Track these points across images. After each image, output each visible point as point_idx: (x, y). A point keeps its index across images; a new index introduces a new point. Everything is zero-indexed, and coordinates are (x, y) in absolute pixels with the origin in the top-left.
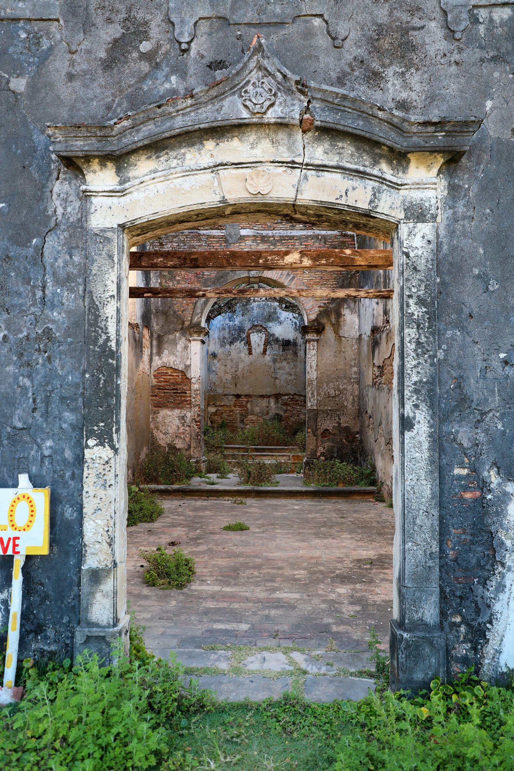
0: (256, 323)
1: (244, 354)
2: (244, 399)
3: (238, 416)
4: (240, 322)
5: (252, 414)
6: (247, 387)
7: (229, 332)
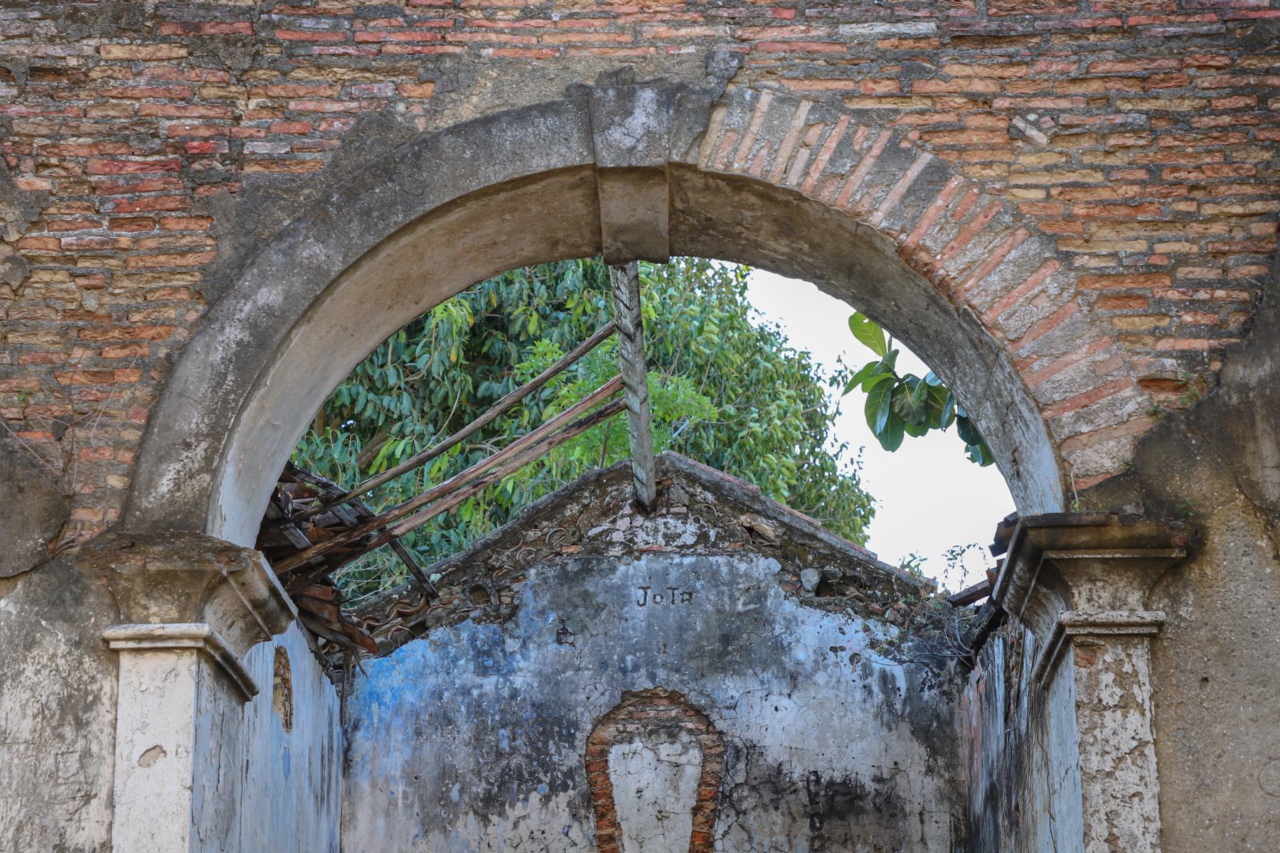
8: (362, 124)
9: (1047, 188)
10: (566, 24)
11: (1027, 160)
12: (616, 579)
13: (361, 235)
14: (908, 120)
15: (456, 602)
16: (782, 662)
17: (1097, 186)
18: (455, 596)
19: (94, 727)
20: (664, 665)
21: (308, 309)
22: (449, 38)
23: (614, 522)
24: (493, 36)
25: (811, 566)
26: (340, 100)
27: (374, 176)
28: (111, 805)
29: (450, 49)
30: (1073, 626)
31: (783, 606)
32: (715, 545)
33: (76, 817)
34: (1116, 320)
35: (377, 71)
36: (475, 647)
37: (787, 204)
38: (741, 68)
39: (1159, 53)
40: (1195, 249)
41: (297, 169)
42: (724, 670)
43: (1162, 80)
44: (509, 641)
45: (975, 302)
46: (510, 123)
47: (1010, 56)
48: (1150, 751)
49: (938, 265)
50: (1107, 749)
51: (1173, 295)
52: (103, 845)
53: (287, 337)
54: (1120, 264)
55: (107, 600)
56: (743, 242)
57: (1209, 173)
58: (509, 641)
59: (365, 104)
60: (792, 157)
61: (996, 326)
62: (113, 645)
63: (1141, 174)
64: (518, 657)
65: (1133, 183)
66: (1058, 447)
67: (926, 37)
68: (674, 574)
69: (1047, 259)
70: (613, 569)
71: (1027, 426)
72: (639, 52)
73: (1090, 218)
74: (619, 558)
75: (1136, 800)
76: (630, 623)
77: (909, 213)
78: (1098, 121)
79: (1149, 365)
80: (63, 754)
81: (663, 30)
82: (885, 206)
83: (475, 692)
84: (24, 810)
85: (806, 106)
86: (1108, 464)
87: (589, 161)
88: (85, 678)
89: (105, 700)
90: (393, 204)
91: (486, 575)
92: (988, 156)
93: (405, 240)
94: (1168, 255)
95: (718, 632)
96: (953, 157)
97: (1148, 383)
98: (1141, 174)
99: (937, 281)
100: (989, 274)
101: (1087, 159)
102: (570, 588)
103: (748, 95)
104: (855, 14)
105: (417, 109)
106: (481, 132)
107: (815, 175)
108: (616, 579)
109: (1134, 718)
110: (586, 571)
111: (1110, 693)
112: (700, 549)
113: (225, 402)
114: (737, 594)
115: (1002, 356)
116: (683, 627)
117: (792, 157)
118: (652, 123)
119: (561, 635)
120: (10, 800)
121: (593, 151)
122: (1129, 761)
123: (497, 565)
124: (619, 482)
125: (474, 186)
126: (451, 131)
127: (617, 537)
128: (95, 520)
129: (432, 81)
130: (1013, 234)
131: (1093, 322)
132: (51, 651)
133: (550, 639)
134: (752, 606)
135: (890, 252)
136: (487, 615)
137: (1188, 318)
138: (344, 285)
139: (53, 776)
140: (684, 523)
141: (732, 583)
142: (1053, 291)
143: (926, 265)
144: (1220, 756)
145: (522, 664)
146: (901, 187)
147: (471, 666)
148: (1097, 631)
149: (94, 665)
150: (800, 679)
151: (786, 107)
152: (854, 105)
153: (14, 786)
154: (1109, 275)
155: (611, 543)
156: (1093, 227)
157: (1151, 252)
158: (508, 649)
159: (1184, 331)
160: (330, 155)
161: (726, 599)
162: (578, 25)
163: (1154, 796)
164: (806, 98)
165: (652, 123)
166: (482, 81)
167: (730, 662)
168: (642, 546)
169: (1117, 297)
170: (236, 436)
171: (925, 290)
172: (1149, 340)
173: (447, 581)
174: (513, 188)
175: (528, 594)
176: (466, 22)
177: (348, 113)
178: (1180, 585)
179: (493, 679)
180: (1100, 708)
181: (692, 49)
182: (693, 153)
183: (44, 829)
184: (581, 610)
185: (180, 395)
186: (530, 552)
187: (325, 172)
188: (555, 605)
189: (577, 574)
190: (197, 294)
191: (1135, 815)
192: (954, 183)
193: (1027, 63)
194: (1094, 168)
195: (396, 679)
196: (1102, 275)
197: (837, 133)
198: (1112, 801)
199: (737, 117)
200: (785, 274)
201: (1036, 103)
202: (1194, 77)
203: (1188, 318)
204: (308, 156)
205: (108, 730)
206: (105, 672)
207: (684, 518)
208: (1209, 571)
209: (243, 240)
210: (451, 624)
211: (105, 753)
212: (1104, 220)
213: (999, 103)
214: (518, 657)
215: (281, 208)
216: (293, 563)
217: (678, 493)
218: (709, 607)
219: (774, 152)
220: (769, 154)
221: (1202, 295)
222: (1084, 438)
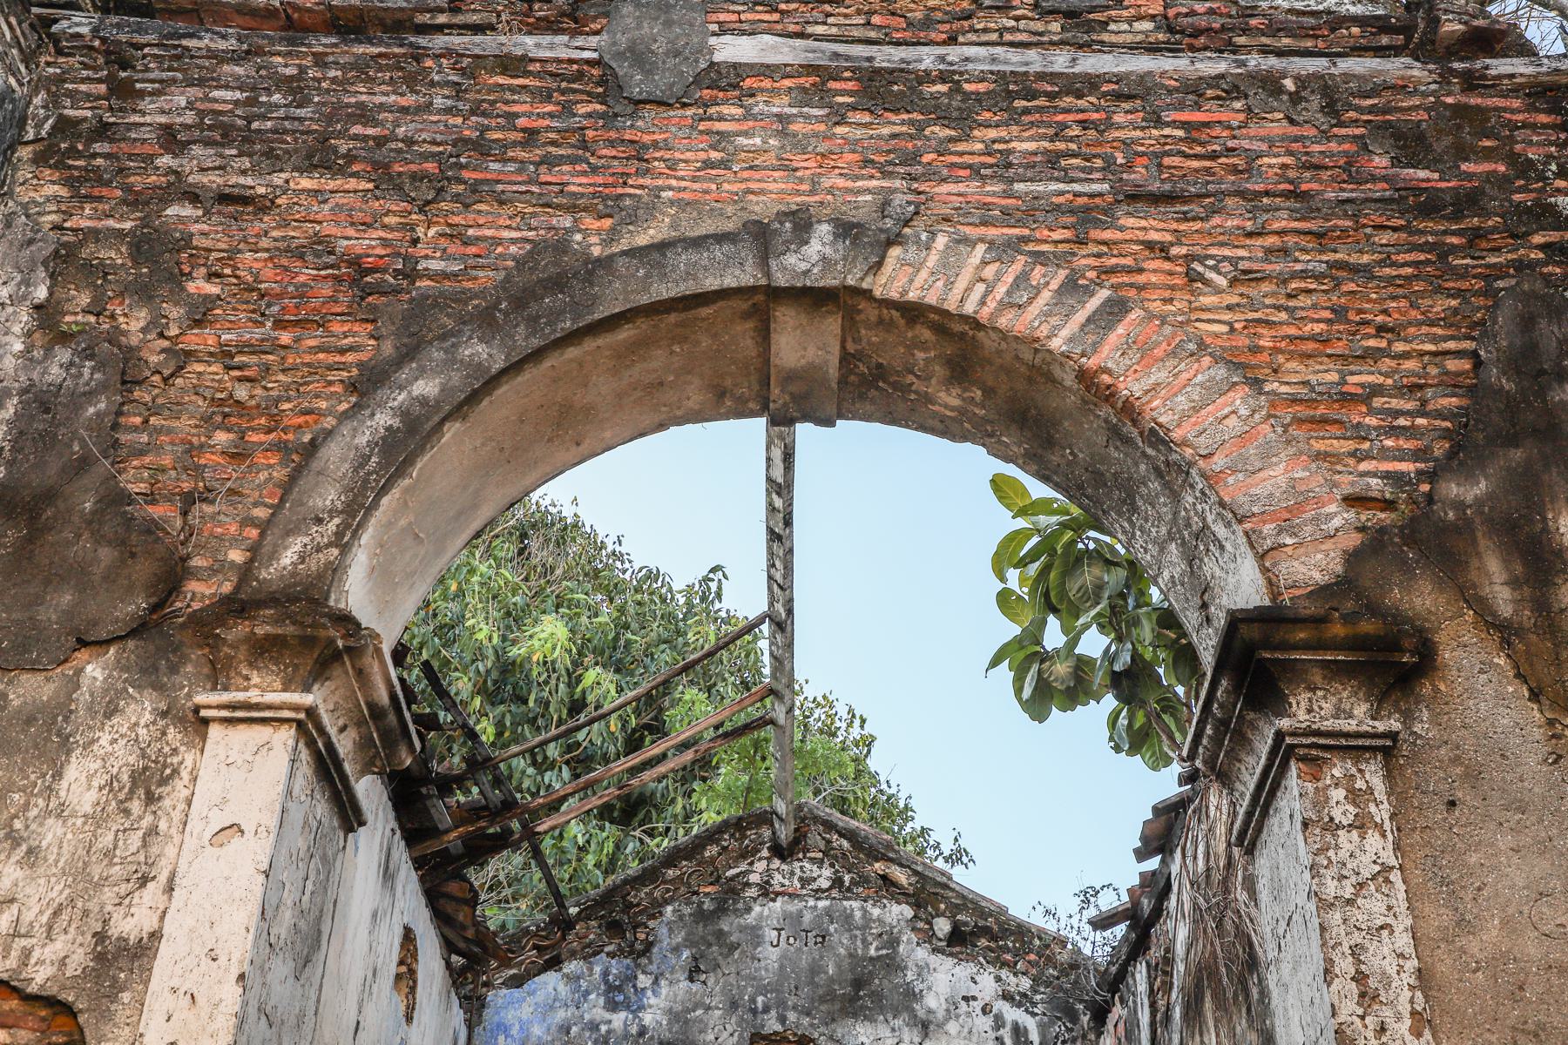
8: (537, 247)
9: (1230, 324)
10: (746, 174)
11: (1206, 300)
12: (750, 919)
13: (527, 338)
14: (1084, 262)
15: (592, 936)
16: (913, 1010)
17: (1281, 323)
18: (592, 931)
19: (167, 803)
20: (794, 1008)
21: (465, 405)
22: (630, 182)
23: (751, 864)
24: (674, 183)
25: (943, 915)
26: (518, 229)
27: (545, 288)
28: (170, 889)
29: (632, 191)
30: (1293, 734)
31: (915, 953)
32: (849, 890)
33: (127, 901)
34: (1312, 442)
35: (558, 207)
36: (607, 982)
37: (963, 335)
38: (917, 213)
39: (1333, 214)
40: (1390, 381)
41: (470, 285)
42: (855, 1015)
43: (1339, 237)
44: (641, 977)
45: (1162, 420)
46: (686, 249)
47: (1184, 213)
48: (1395, 876)
49: (1122, 386)
50: (1345, 872)
51: (1371, 421)
52: (152, 935)
53: (438, 428)
54: (1312, 390)
55: (206, 670)
56: (913, 397)
57: (1396, 316)
58: (641, 977)
59: (542, 232)
60: (968, 290)
61: (1185, 443)
62: (203, 713)
63: (1327, 314)
64: (649, 993)
65: (1318, 321)
66: (1261, 557)
67: (1101, 195)
68: (808, 917)
69: (1235, 384)
70: (749, 910)
71: (1222, 548)
72: (817, 198)
73: (1276, 350)
74: (755, 900)
75: (1385, 933)
76: (763, 964)
77: (1091, 339)
78: (1277, 267)
79: (1352, 484)
80: (125, 830)
81: (841, 182)
82: (1065, 333)
83: (604, 1028)
84: (67, 891)
85: (981, 248)
86: (1317, 576)
87: (763, 282)
88: (167, 749)
89: (185, 774)
90: (563, 312)
91: (623, 911)
92: (1167, 294)
93: (572, 352)
94: (1362, 385)
95: (850, 976)
96: (1132, 293)
97: (1352, 501)
98: (1327, 314)
99: (1120, 404)
100: (1175, 395)
101: (1268, 301)
102: (705, 926)
103: (924, 236)
104: (1029, 174)
105: (594, 240)
106: (656, 256)
107: (992, 305)
108: (750, 919)
109: (1373, 841)
110: (721, 910)
111: (1342, 812)
112: (835, 893)
113: (366, 481)
114: (870, 939)
115: (1193, 472)
116: (815, 969)
117: (968, 290)
118: (828, 251)
119: (693, 973)
120: (53, 880)
121: (768, 274)
122: (1372, 887)
123: (635, 901)
124: (758, 826)
125: (645, 300)
126: (624, 253)
127: (754, 878)
128: (208, 592)
129: (611, 216)
130: (1198, 361)
131: (1288, 442)
132: (133, 720)
133: (682, 976)
134: (884, 952)
135: (1069, 380)
136: (621, 950)
137: (1389, 443)
138: (504, 388)
139: (109, 854)
140: (820, 868)
141: (865, 927)
142: (1244, 412)
143: (1109, 387)
144: (1479, 889)
145: (653, 1001)
146: (1081, 316)
147: (602, 1001)
148: (1322, 741)
149: (179, 736)
150: (932, 1027)
151: (961, 247)
152: (1031, 247)
153: (61, 864)
154: (1301, 400)
155: (748, 884)
156: (1281, 359)
157: (1343, 382)
158: (640, 985)
159: (1384, 455)
160: (503, 273)
161: (859, 943)
162: (757, 175)
163: (1406, 930)
164: (982, 240)
165: (828, 251)
166: (660, 218)
167: (861, 1007)
168: (778, 888)
169: (1312, 420)
170: (373, 520)
171: (1106, 421)
172: (1351, 461)
173: (585, 915)
174: (686, 309)
175: (664, 930)
176: (648, 170)
177: (526, 240)
178: (1412, 699)
179: (623, 1015)
180: (1332, 826)
181: (869, 198)
182: (869, 279)
183: (86, 913)
184: (715, 948)
185: (319, 473)
186: (668, 890)
187: (495, 287)
188: (689, 942)
189: (713, 912)
190: (352, 387)
191: (1386, 951)
192: (1133, 315)
193: (1202, 219)
194: (1278, 308)
195: (526, 1011)
196: (1295, 400)
197: (1017, 267)
198: (1356, 933)
199: (912, 253)
200: (953, 438)
201: (1213, 251)
202: (1371, 236)
203: (1389, 443)
204: (481, 274)
205: (182, 806)
206: (190, 745)
207: (820, 863)
208: (1442, 687)
209: (405, 340)
210: (585, 958)
211: (173, 831)
212: (1290, 352)
213: (1174, 251)
214: (649, 993)
215: (448, 315)
216: (431, 847)
217: (815, 838)
218: (842, 951)
219: (949, 285)
220: (945, 285)
221: (1402, 422)
222: (1289, 550)
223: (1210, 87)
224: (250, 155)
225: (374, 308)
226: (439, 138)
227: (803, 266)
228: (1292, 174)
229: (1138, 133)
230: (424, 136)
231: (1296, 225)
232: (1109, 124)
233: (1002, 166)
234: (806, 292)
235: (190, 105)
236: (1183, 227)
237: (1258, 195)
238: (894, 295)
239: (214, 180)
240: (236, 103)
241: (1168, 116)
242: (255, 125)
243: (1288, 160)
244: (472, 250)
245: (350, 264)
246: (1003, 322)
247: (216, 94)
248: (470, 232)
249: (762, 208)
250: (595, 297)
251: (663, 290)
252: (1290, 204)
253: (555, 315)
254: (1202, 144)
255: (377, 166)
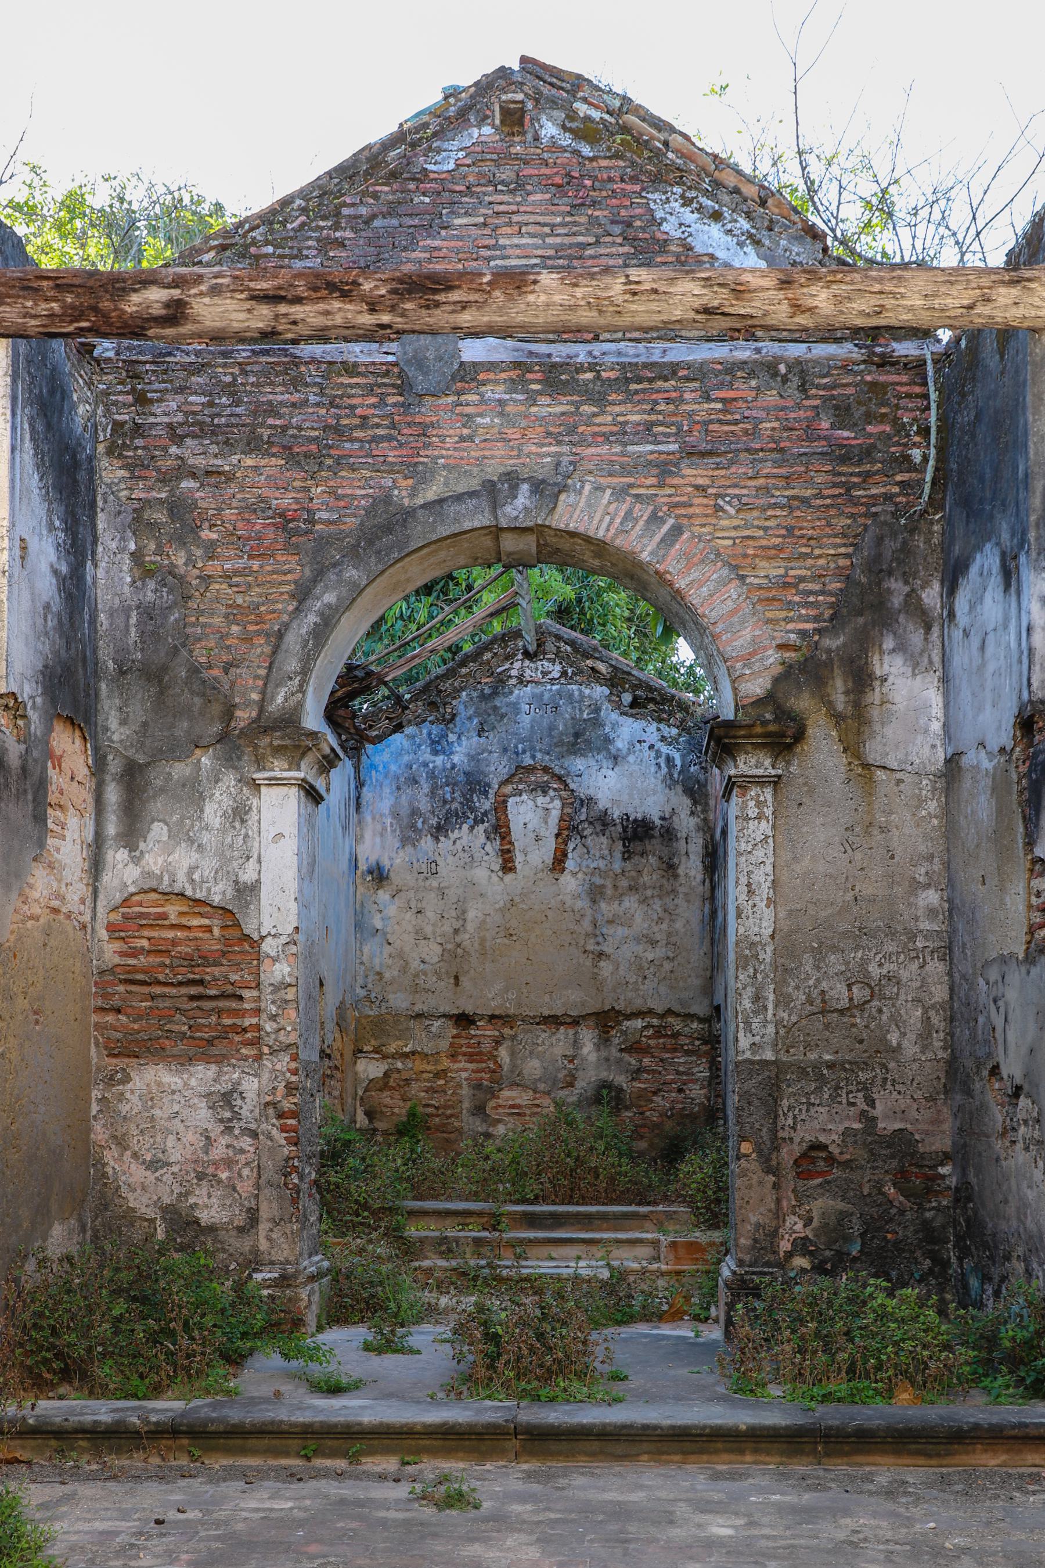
0: (528, 761)
1: (485, 872)
2: (485, 1032)
3: (465, 1091)
4: (473, 758)
5: (514, 1084)
6: (498, 986)
7: (433, 793)
11: (725, 523)
14: (662, 500)
41: (343, 527)
60: (601, 521)
85: (609, 492)
92: (704, 521)
96: (685, 521)
101: (756, 523)
106: (438, 508)
107: (612, 531)
117: (601, 521)
118: (527, 502)
121: (496, 518)
125: (434, 537)
126: (422, 507)
146: (657, 538)
152: (634, 491)
177: (368, 495)
197: (625, 507)
201: (730, 491)
204: (348, 520)
223: (739, 369)
224: (217, 444)
225: (297, 546)
226: (315, 425)
227: (515, 513)
228: (777, 434)
229: (696, 407)
230: (307, 424)
231: (775, 471)
232: (681, 400)
233: (621, 434)
234: (516, 528)
235: (179, 409)
236: (717, 473)
237: (757, 451)
238: (562, 526)
239: (200, 462)
240: (203, 404)
241: (714, 394)
242: (216, 421)
243: (776, 425)
244: (342, 504)
245: (281, 515)
246: (618, 542)
247: (191, 399)
248: (340, 491)
249: (493, 470)
250: (409, 537)
251: (444, 531)
252: (775, 456)
253: (390, 549)
254: (732, 414)
255: (284, 447)
